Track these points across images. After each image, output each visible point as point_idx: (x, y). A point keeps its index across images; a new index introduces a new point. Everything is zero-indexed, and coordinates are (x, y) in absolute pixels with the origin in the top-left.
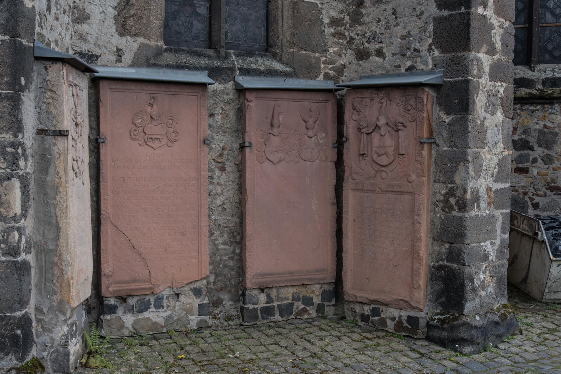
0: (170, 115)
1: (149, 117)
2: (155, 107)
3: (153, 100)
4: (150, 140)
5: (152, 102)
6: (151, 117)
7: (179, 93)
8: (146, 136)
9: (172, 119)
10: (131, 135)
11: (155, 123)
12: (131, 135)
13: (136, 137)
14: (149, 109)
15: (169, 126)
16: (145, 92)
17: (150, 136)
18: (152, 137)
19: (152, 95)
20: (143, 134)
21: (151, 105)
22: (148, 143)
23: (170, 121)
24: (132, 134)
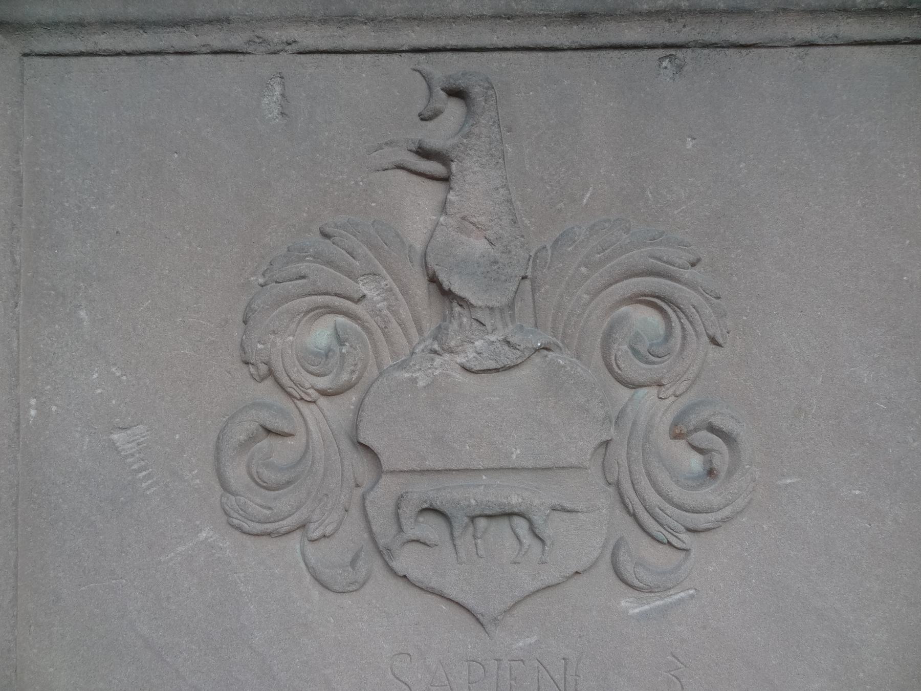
0: (639, 256)
1: (420, 288)
2: (476, 182)
3: (454, 109)
4: (431, 528)
5: (438, 135)
6: (433, 279)
7: (732, 31)
8: (389, 486)
9: (655, 301)
10: (225, 487)
11: (478, 347)
12: (225, 487)
13: (284, 502)
14: (416, 207)
15: (633, 368)
16: (368, 37)
17: (424, 490)
18: (447, 493)
19: (445, 68)
20: (360, 466)
21: (435, 164)
22: (407, 560)
23: (646, 319)
24: (237, 474)
